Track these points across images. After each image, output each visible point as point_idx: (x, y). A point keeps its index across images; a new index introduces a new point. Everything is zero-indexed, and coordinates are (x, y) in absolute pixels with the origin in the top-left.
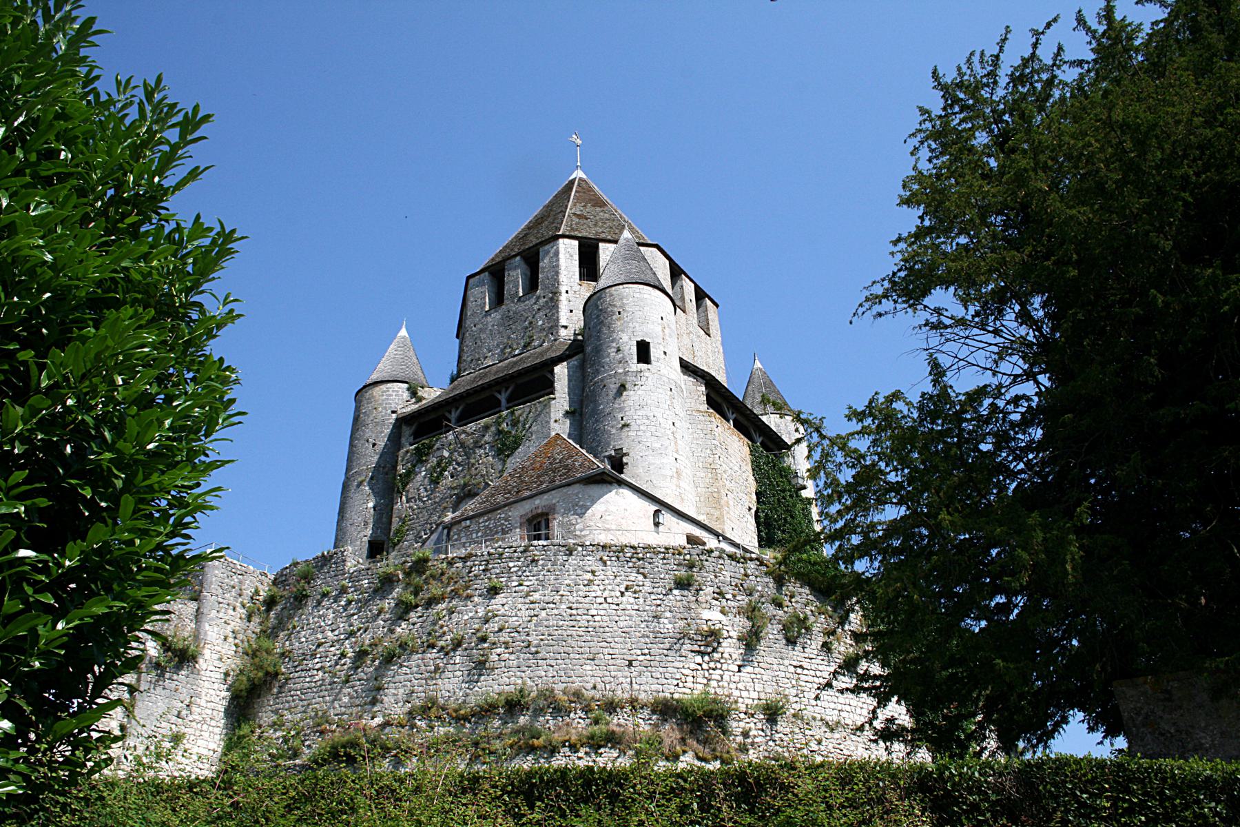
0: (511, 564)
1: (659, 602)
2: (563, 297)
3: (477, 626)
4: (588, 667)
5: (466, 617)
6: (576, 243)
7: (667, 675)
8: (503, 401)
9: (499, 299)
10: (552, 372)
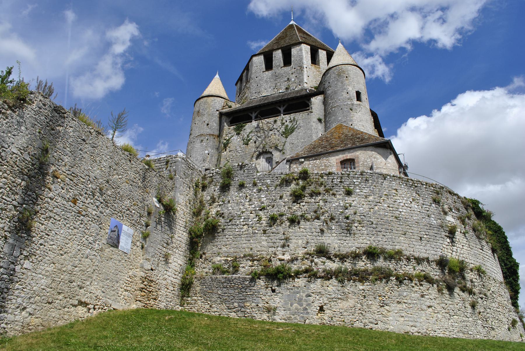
0: (355, 181)
1: (428, 209)
2: (305, 69)
3: (341, 211)
4: (402, 239)
5: (334, 205)
6: (309, 47)
7: (438, 247)
8: (282, 111)
9: (269, 66)
10: (309, 100)
